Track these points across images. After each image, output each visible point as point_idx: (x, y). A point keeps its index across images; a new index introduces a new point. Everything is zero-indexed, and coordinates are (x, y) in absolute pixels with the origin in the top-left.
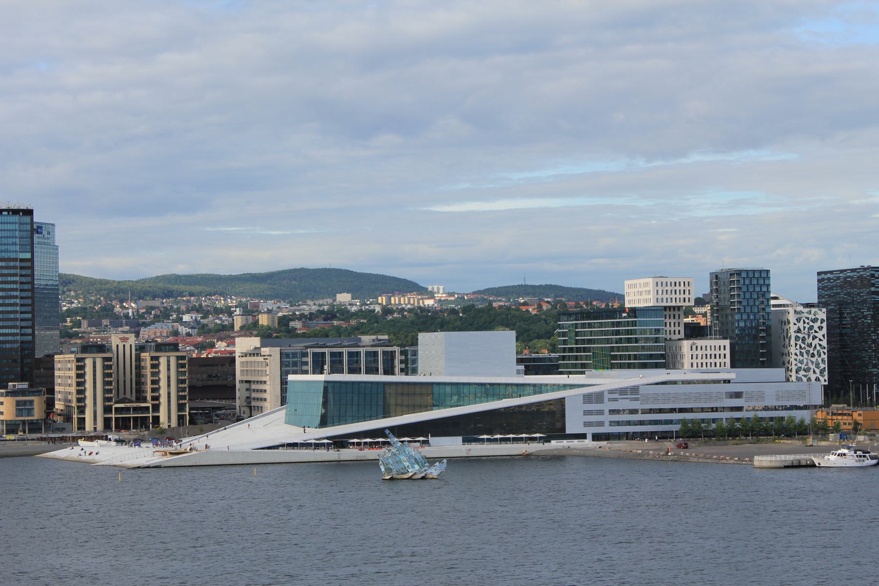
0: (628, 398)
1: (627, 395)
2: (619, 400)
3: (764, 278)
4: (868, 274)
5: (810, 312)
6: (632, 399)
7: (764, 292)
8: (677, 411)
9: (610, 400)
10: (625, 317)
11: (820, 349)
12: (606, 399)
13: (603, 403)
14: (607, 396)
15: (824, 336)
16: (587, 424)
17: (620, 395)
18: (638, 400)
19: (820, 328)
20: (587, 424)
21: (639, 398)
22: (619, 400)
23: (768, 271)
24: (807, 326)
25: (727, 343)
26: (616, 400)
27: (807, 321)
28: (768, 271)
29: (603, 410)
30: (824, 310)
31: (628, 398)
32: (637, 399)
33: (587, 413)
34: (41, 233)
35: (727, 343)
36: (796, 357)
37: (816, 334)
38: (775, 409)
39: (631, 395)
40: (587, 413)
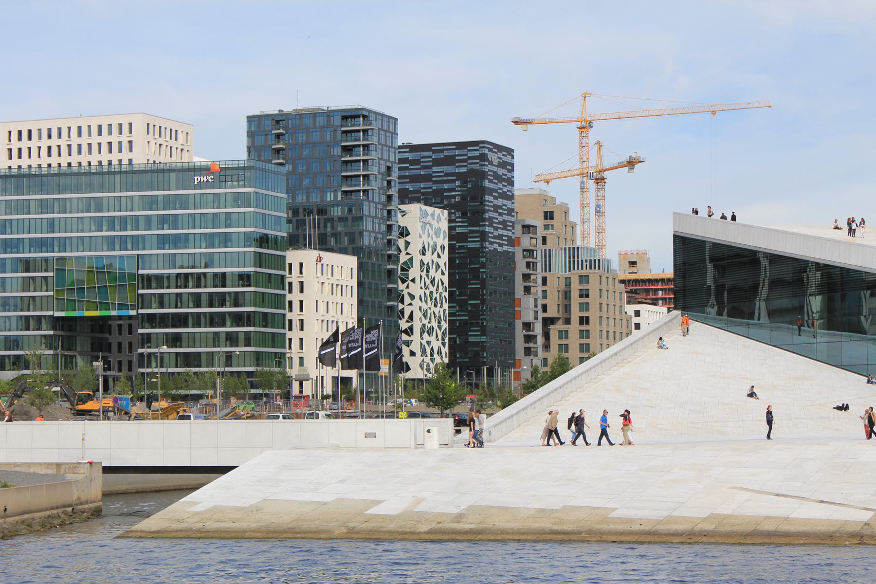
3: (392, 133)
4: (477, 154)
5: (433, 215)
7: (392, 162)
10: (200, 185)
11: (442, 291)
15: (445, 264)
19: (443, 247)
23: (396, 120)
24: (431, 243)
25: (352, 261)
27: (431, 233)
28: (396, 120)
30: (446, 212)
35: (352, 261)
36: (420, 304)
37: (439, 260)
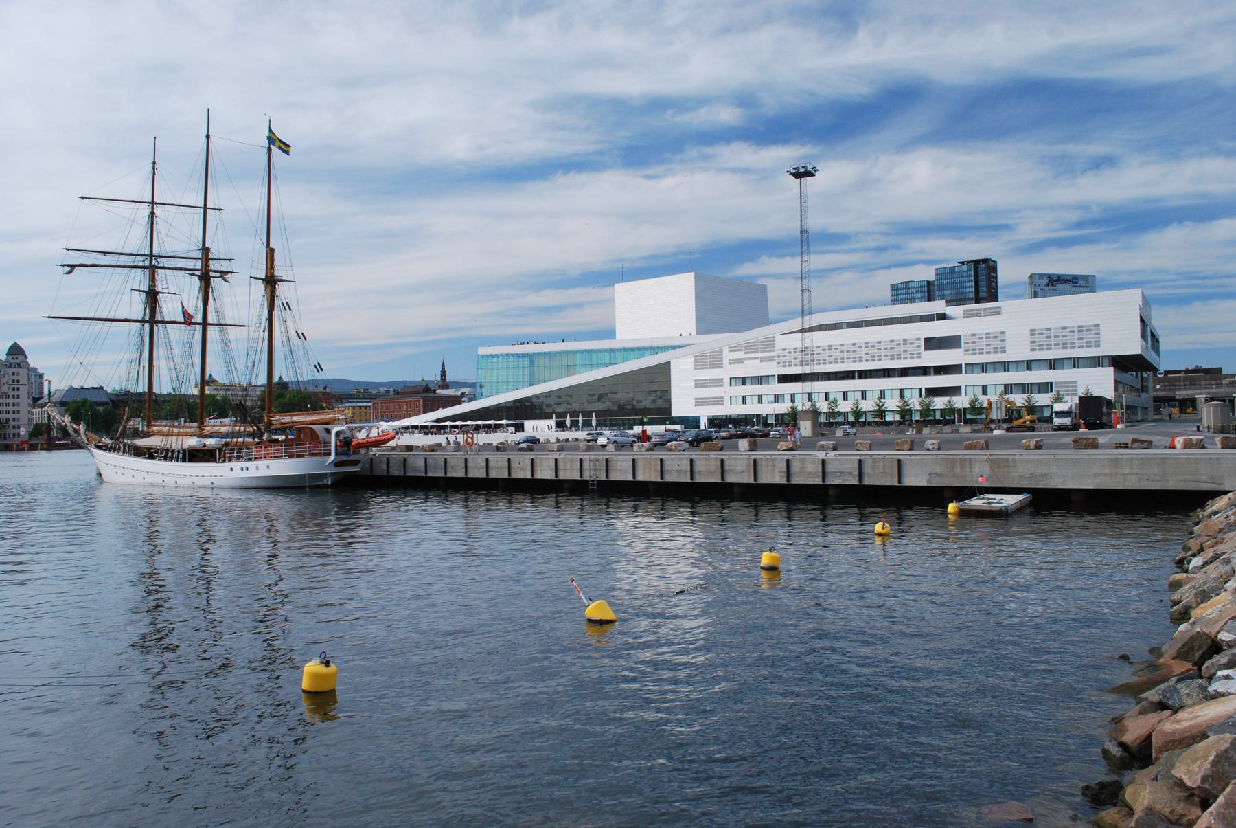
0: (757, 358)
1: (757, 352)
2: (745, 362)
6: (763, 360)
8: (856, 375)
9: (732, 362)
12: (726, 362)
13: (722, 367)
14: (727, 356)
16: (700, 402)
17: (745, 353)
18: (774, 360)
20: (700, 402)
21: (774, 357)
22: (745, 362)
26: (740, 361)
29: (722, 379)
31: (757, 358)
32: (771, 359)
33: (700, 384)
34: (1077, 283)
38: (1029, 365)
39: (762, 352)
40: (700, 384)
